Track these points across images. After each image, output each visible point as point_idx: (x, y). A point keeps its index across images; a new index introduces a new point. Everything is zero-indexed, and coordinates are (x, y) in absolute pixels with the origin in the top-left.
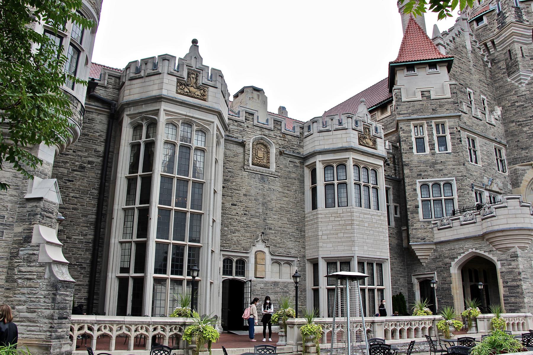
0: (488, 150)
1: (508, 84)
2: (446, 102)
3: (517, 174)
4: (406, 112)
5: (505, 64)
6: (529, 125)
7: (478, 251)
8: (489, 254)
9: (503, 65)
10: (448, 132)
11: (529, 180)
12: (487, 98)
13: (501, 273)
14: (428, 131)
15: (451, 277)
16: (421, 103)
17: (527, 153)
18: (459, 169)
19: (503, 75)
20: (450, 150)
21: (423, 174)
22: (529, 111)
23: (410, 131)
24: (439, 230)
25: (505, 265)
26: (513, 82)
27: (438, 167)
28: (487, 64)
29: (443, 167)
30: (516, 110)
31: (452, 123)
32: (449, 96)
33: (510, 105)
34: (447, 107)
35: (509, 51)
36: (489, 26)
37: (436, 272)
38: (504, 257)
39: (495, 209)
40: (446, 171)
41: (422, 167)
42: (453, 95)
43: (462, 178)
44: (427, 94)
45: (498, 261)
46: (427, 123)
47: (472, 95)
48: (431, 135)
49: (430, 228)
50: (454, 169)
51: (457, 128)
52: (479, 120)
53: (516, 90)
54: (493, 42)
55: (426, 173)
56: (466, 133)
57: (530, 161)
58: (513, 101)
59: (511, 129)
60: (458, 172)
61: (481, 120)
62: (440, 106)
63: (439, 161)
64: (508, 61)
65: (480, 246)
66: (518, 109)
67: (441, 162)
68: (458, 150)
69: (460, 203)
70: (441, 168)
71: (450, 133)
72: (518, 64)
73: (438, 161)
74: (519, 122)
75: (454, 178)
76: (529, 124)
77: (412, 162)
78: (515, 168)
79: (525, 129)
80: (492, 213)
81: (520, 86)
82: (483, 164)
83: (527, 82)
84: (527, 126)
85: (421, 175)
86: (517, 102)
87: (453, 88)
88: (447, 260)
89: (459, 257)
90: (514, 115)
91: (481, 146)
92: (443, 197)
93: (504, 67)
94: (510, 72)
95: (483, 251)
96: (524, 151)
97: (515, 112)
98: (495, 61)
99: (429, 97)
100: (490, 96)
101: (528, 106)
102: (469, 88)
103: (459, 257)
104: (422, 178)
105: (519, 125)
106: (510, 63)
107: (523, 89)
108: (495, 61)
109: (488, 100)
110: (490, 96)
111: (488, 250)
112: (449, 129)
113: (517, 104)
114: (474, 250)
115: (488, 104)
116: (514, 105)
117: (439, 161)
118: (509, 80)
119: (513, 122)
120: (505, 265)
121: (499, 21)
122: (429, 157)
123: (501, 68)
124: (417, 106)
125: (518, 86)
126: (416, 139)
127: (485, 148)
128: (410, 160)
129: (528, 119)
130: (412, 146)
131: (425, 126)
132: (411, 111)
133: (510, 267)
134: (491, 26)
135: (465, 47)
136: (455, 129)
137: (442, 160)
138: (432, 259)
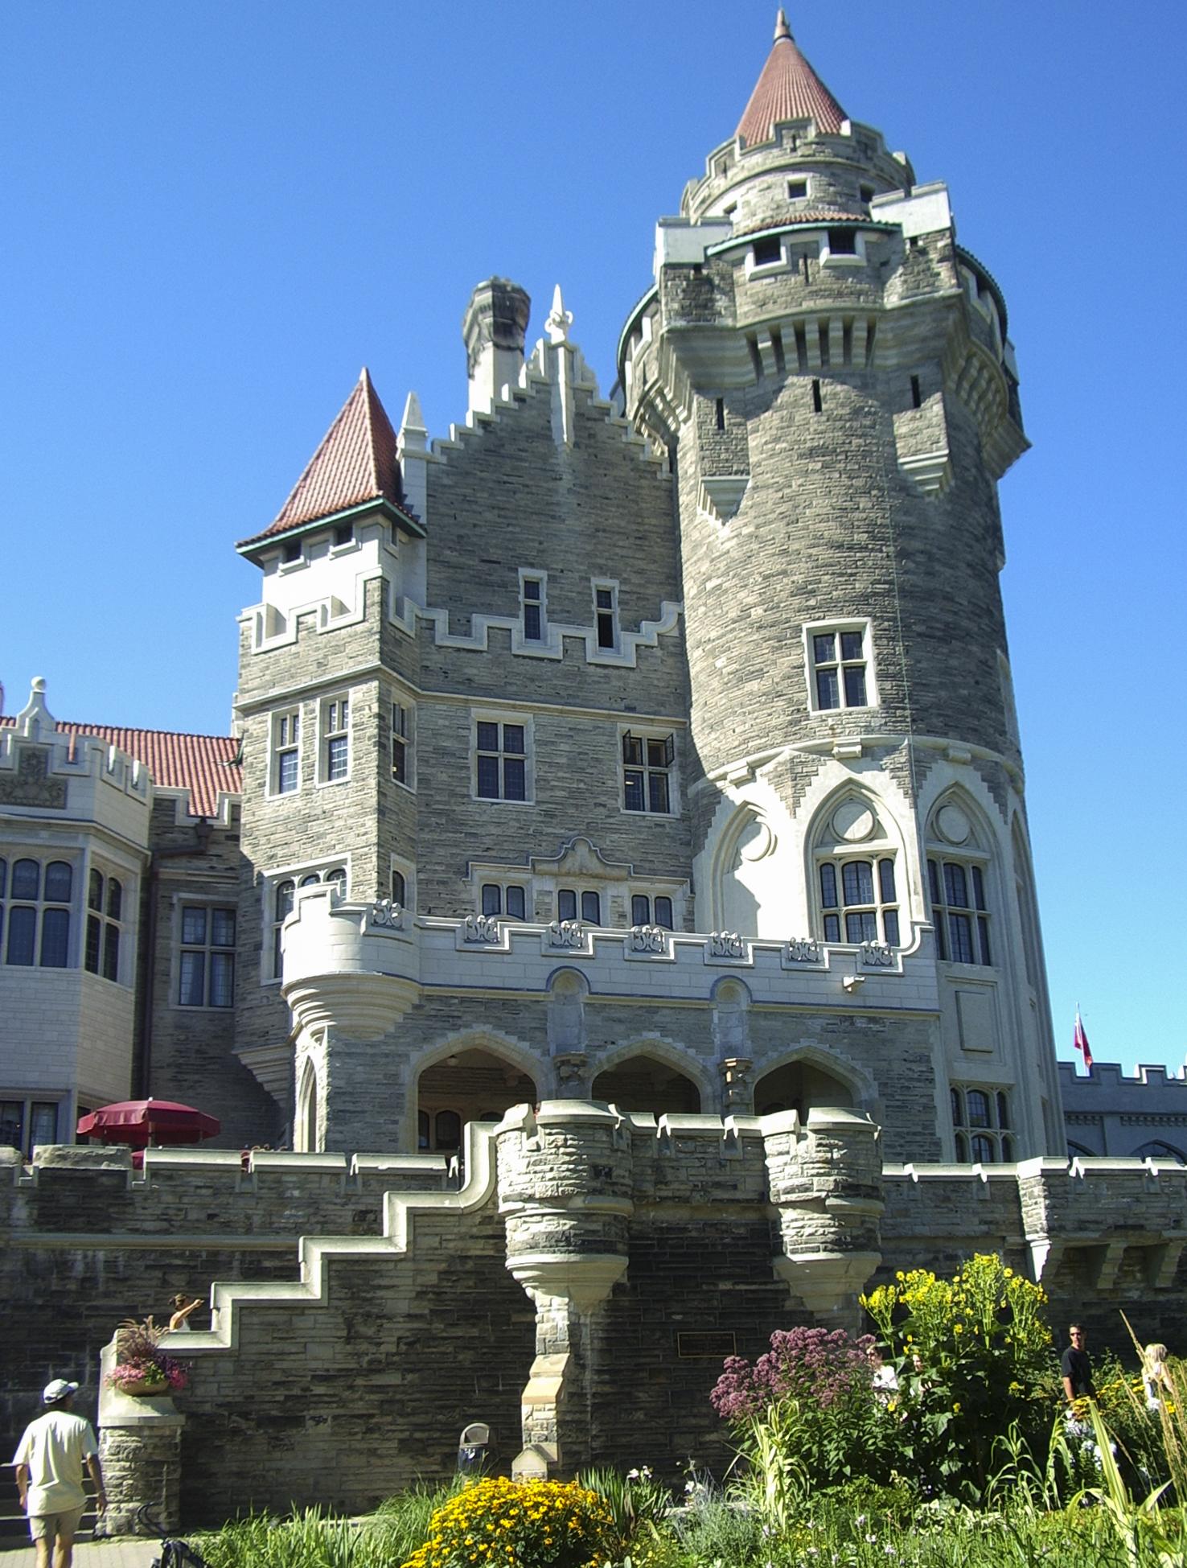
10: (350, 720)
12: (624, 582)
18: (363, 825)
21: (280, 853)
27: (316, 827)
31: (360, 695)
43: (366, 849)
47: (543, 590)
51: (370, 709)
62: (338, 649)
63: (319, 811)
79: (719, 663)
82: (544, 796)
86: (709, 579)
100: (641, 572)
102: (532, 565)
110: (641, 572)
113: (710, 585)
117: (319, 811)
122: (299, 803)
127: (563, 747)
132: (267, 678)
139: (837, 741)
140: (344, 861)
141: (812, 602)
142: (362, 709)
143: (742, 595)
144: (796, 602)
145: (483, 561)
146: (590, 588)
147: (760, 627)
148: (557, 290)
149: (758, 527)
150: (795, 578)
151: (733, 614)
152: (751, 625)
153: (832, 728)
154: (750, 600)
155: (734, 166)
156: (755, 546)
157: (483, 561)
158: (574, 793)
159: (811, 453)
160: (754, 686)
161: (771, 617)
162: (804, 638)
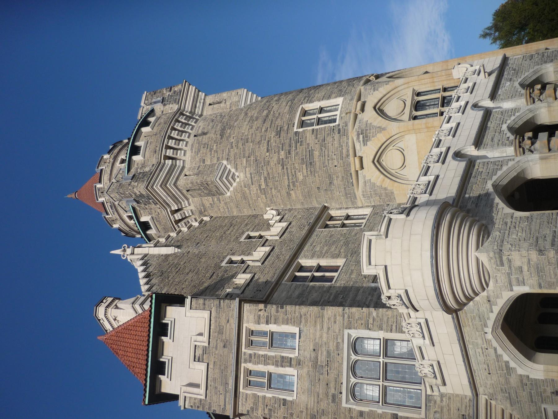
0: (323, 241)
1: (233, 196)
2: (216, 321)
3: (371, 194)
4: (222, 397)
5: (206, 198)
6: (295, 171)
7: (490, 323)
8: (496, 304)
9: (208, 201)
11: (382, 176)
12: (248, 230)
13: (540, 286)
14: (259, 363)
15: (553, 380)
16: (211, 366)
17: (337, 177)
18: (329, 319)
19: (222, 202)
20: (296, 330)
22: (274, 170)
23: (256, 397)
24: (444, 384)
25: (521, 279)
26: (231, 189)
27: (322, 358)
28: (203, 222)
29: (324, 349)
30: (271, 189)
31: (251, 317)
32: (206, 314)
33: (264, 196)
34: (223, 321)
35: (188, 191)
36: (153, 215)
37: (543, 406)
38: (502, 279)
39: (389, 288)
40: (331, 344)
41: (321, 390)
42: (206, 306)
43: (346, 316)
44: (199, 352)
45: (512, 290)
46: (245, 361)
48: (266, 360)
49: (442, 400)
50: (329, 329)
51: (260, 310)
52: (272, 253)
53: (243, 186)
54: (177, 211)
55: (332, 385)
56: (283, 282)
57: (351, 174)
58: (259, 191)
59: (301, 198)
60: (335, 322)
61: (273, 248)
62: (221, 332)
64: (202, 194)
65: (477, 319)
66: (270, 184)
67: (314, 350)
68: (297, 314)
69: (394, 328)
70: (325, 353)
71: (267, 323)
72: (205, 182)
73: (312, 356)
74: (289, 186)
75: (346, 332)
76: (293, 171)
77: (309, 406)
78: (362, 196)
79: (301, 178)
80: (400, 296)
81: (238, 180)
82: (343, 255)
83: (233, 170)
84: (295, 174)
85: (334, 396)
86: (260, 186)
87: (196, 303)
88: (513, 380)
89: (506, 358)
90: (279, 191)
91: (312, 257)
92: (381, 360)
93: (210, 198)
94: (217, 192)
95: (491, 314)
96: (335, 182)
97: (275, 189)
98: (203, 211)
99: (205, 349)
100: (246, 225)
101: (267, 171)
102: (222, 261)
103: (506, 358)
104: (340, 396)
105: (294, 185)
106: (205, 192)
107: (242, 175)
108: (203, 211)
109: (251, 229)
110: (246, 225)
111: (488, 305)
112: (259, 324)
113: (263, 186)
114: (489, 330)
115: (257, 231)
116: (264, 191)
117: (313, 355)
118: (229, 194)
119: (289, 194)
120: (521, 279)
121: (146, 202)
123: (212, 203)
124: (215, 373)
125: (238, 183)
126: (270, 387)
128: (305, 411)
129: (286, 172)
130: (280, 399)
131: (251, 366)
133: (525, 268)
134: (153, 211)
135: (167, 256)
136: (261, 313)
137: (312, 348)
138: (511, 405)
139: (353, 111)
140: (349, 336)
141: (286, 128)
142: (259, 317)
143: (272, 164)
144: (283, 134)
145: (210, 278)
146: (245, 241)
147: (289, 153)
148: (113, 252)
149: (244, 157)
150: (272, 136)
151: (280, 168)
152: (287, 158)
153: (347, 114)
154: (275, 159)
155: (104, 188)
156: (252, 158)
157: (210, 278)
158: (347, 244)
159: (222, 136)
160: (316, 153)
161: (287, 147)
162: (301, 130)
